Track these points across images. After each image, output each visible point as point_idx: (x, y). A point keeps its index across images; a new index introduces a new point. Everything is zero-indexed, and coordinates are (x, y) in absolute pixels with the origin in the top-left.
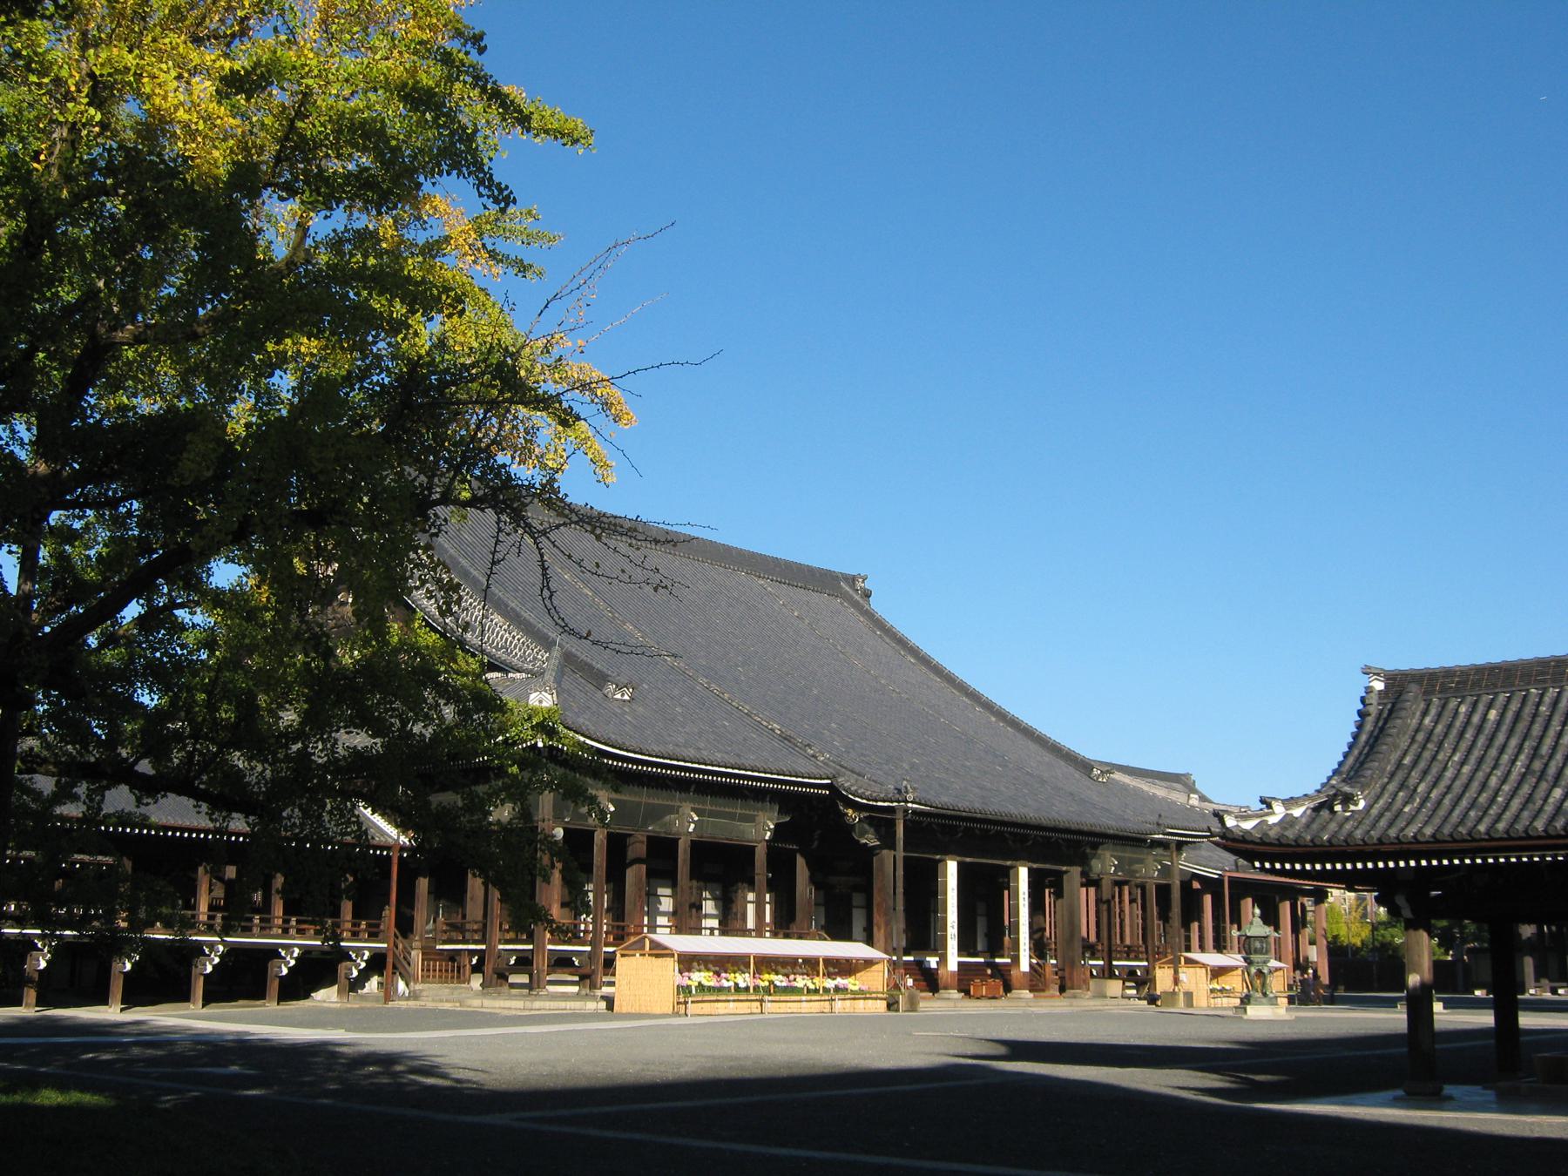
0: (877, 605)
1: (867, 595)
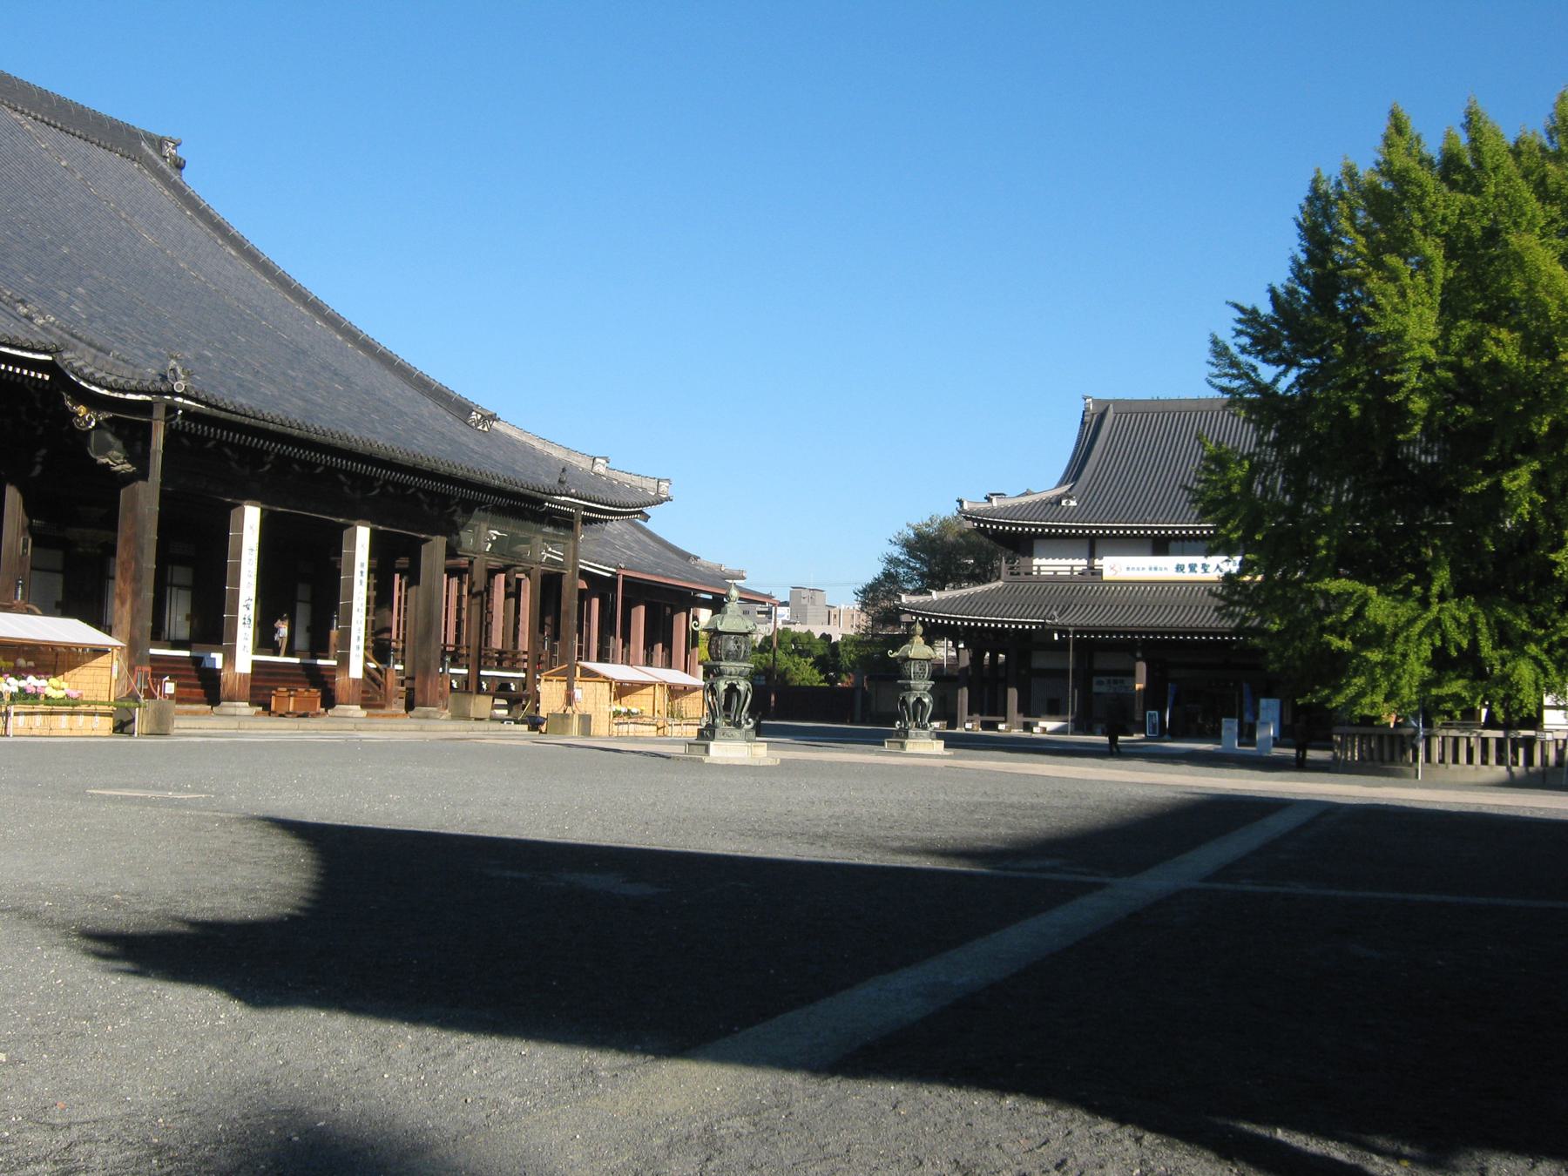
0: (189, 177)
1: (179, 165)
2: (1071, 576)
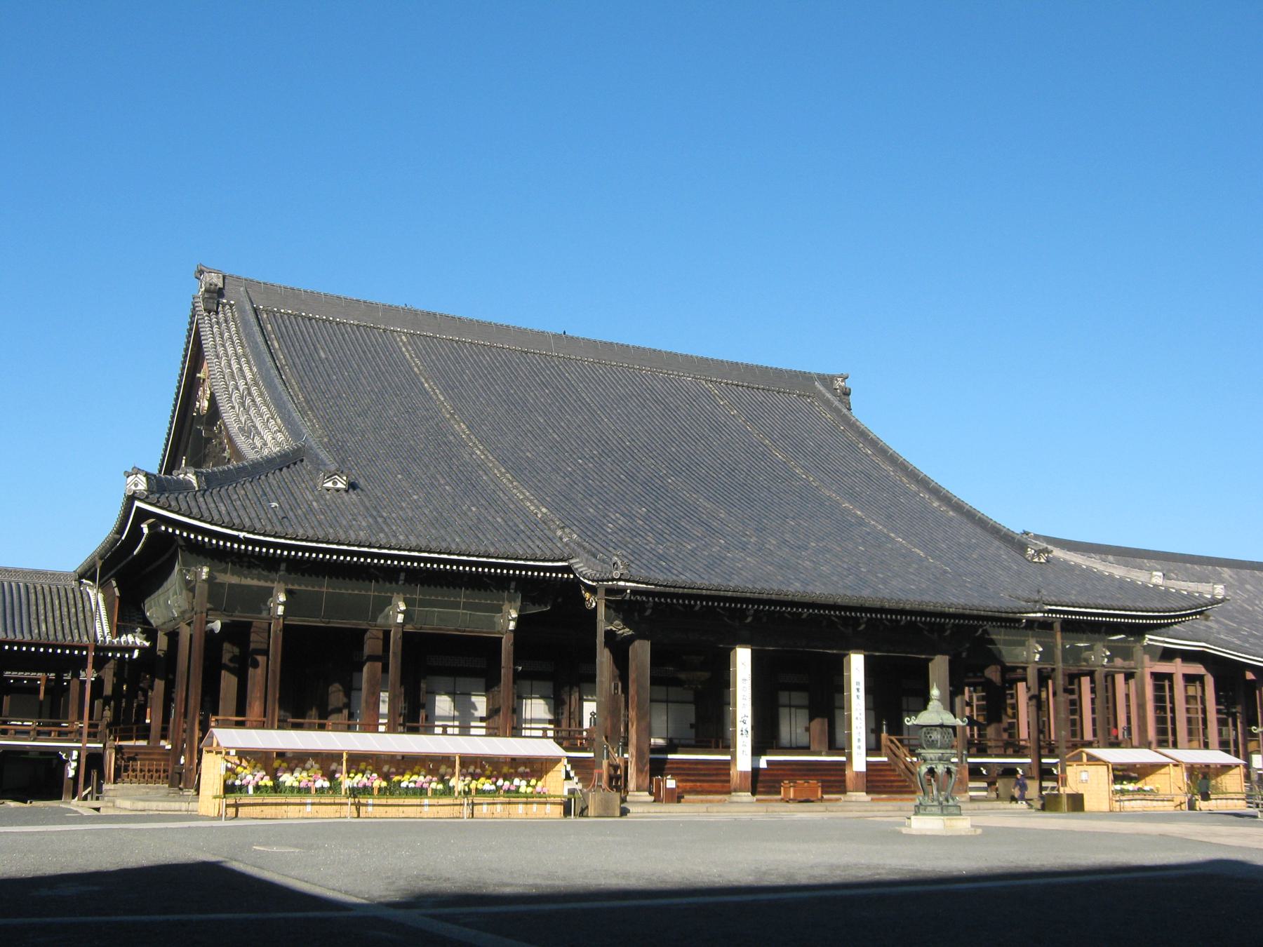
1: (847, 393)
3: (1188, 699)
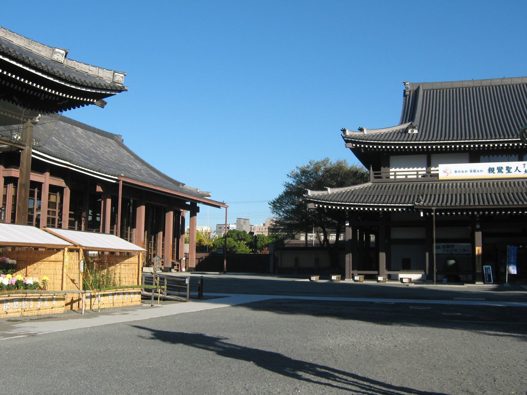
2: (417, 178)
3: (51, 205)
